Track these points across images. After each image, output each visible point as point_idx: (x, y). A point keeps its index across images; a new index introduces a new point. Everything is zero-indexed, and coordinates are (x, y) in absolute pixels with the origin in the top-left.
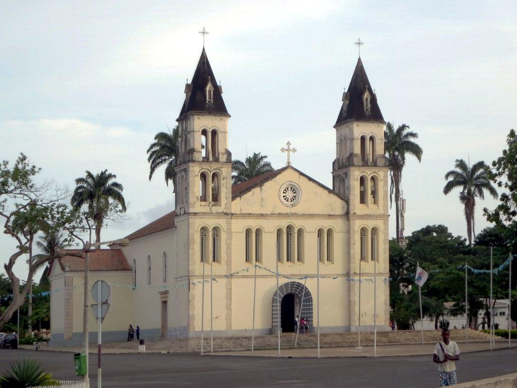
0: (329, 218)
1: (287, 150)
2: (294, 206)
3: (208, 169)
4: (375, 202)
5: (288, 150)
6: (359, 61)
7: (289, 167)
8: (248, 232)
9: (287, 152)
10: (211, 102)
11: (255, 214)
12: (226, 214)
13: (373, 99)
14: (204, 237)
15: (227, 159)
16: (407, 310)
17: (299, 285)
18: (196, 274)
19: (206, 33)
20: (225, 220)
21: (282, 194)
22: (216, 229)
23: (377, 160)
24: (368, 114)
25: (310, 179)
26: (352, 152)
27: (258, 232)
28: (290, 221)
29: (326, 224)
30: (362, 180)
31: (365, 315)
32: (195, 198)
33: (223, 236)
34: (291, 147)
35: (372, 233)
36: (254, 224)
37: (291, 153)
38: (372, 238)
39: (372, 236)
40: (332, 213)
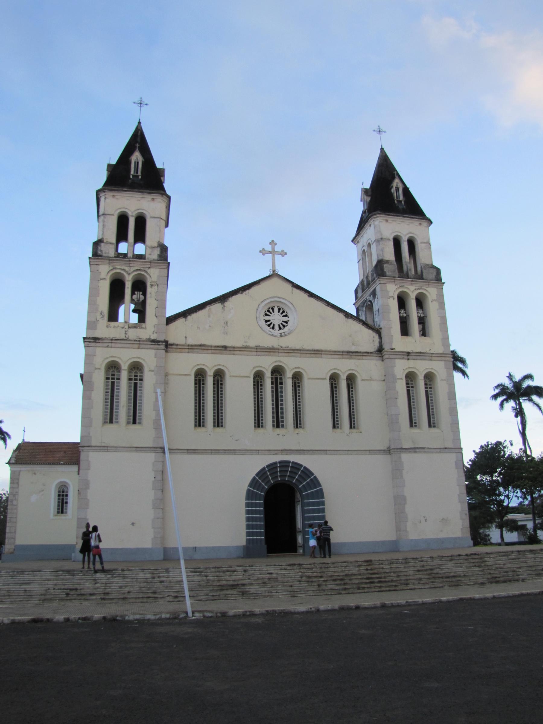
0: (349, 356)
1: (270, 252)
2: (285, 335)
3: (124, 270)
4: (424, 333)
5: (273, 252)
6: (381, 152)
7: (274, 275)
9: (271, 255)
10: (138, 176)
11: (211, 346)
12: (153, 341)
13: (406, 191)
14: (116, 381)
16: (505, 496)
17: (296, 466)
18: (93, 443)
20: (153, 351)
21: (263, 318)
23: (424, 271)
24: (400, 207)
25: (311, 295)
26: (380, 258)
27: (219, 376)
28: (278, 358)
30: (402, 302)
31: (426, 521)
32: (99, 314)
34: (277, 249)
35: (426, 384)
37: (277, 257)
38: (427, 392)
39: (426, 388)
40: (353, 349)
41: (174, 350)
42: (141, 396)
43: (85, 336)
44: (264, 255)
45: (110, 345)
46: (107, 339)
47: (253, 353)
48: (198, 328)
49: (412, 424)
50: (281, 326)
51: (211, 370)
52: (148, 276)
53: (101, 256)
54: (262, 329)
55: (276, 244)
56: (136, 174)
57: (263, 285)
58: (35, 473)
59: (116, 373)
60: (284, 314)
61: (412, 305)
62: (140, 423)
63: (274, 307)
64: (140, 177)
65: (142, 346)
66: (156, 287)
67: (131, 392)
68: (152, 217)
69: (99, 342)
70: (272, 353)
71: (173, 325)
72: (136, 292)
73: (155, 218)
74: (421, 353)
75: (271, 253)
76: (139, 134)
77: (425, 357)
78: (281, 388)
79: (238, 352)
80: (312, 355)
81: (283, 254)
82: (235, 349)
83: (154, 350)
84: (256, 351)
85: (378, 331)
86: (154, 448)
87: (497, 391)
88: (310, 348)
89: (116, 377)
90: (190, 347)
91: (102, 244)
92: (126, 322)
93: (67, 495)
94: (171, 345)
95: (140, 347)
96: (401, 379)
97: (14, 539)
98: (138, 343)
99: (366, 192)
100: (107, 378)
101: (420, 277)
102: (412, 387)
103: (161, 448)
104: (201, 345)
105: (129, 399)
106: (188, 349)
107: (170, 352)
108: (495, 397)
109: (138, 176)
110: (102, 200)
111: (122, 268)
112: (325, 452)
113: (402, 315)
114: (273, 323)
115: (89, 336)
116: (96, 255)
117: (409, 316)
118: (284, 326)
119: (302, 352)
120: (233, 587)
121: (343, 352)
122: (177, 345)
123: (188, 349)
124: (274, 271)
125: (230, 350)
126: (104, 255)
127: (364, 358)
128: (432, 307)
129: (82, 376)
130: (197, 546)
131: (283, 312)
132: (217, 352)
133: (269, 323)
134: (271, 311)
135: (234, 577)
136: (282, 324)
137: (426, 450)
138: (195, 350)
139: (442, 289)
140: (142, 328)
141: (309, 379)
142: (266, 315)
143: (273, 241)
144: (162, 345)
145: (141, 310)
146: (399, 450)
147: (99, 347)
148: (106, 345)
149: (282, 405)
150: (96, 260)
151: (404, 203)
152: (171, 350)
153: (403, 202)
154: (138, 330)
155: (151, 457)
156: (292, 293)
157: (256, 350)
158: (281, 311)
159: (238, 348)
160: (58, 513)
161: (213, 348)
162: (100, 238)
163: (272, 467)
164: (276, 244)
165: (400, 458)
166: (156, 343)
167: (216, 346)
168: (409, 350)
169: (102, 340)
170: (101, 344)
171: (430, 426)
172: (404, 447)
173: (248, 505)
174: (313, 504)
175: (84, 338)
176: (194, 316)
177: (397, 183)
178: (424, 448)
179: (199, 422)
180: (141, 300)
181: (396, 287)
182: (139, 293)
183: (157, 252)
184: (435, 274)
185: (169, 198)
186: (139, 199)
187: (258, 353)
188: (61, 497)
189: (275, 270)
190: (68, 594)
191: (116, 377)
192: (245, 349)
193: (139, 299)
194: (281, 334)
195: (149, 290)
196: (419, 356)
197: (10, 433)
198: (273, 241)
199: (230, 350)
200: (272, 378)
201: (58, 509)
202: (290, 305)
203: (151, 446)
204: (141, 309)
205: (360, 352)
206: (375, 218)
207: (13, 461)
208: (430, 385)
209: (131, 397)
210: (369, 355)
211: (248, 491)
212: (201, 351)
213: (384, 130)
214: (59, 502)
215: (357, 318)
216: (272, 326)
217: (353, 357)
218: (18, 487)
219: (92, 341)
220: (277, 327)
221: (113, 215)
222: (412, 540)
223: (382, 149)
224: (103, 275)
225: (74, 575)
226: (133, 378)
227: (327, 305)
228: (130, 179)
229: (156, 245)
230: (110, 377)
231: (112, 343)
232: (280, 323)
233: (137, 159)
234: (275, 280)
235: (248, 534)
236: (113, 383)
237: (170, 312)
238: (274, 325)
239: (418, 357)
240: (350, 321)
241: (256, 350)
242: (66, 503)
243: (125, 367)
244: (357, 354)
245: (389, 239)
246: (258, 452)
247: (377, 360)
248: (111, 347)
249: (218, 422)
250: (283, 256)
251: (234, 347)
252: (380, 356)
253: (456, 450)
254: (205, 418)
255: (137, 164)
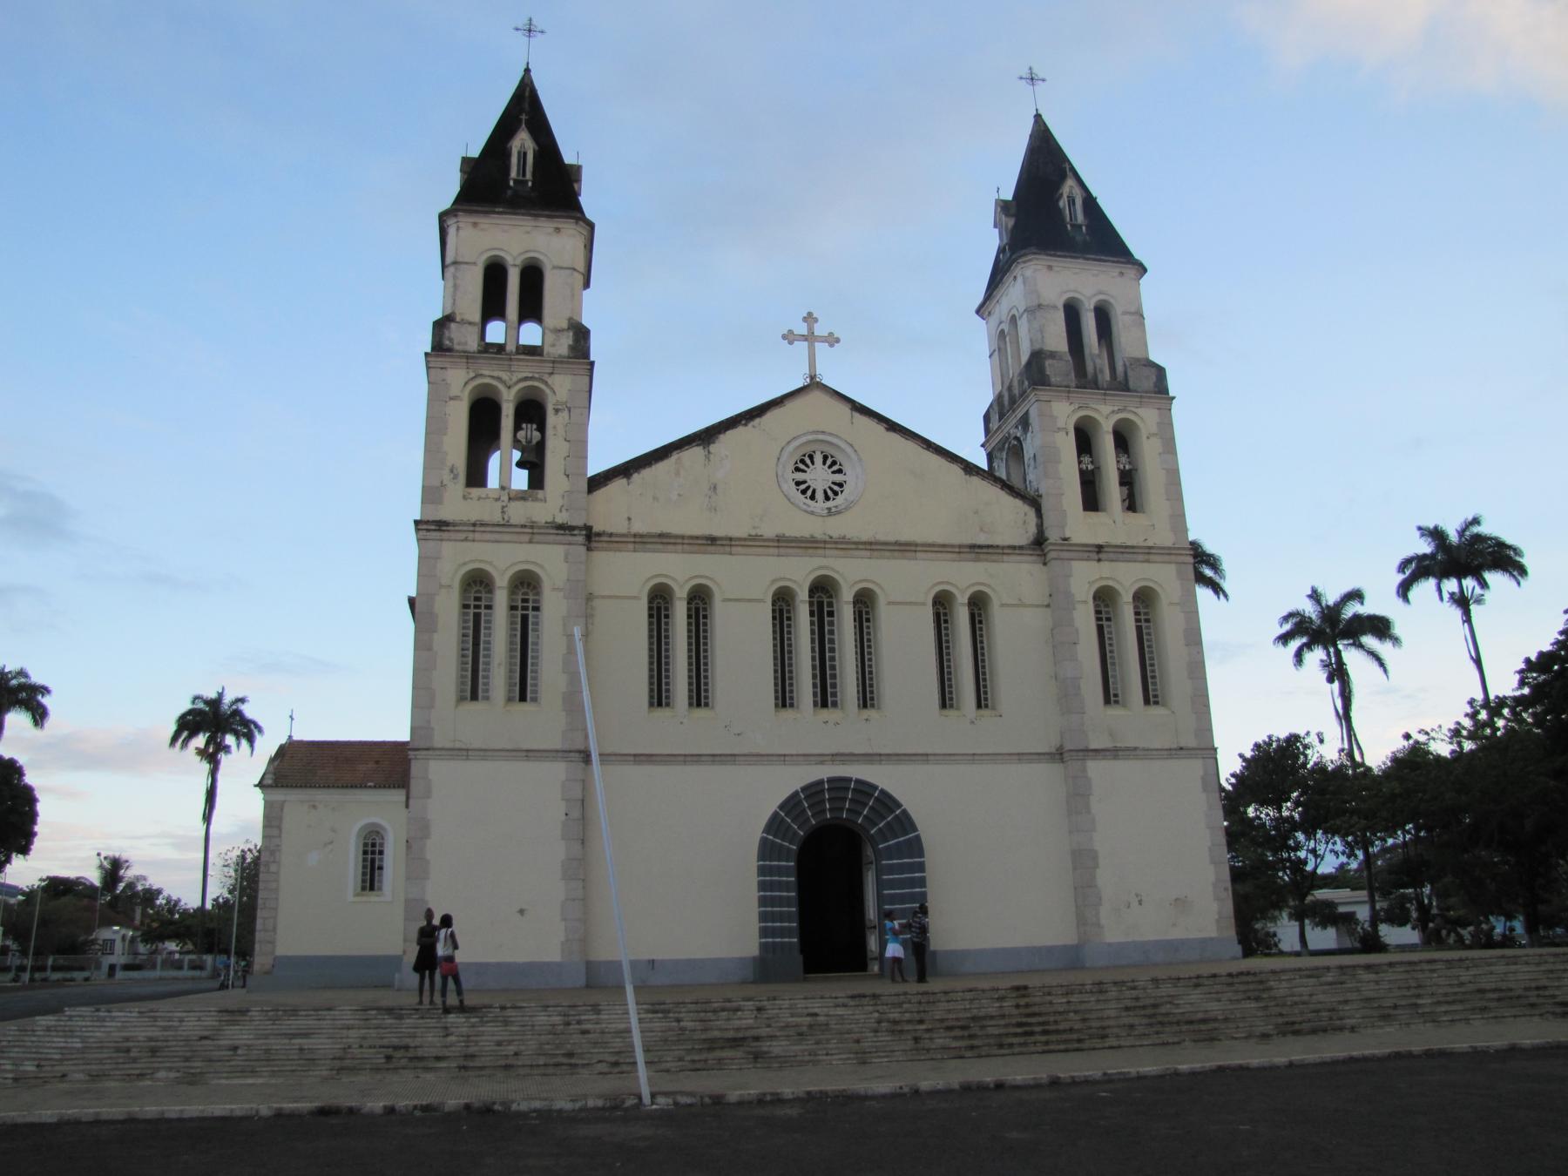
0: (973, 555)
1: (804, 338)
2: (839, 513)
3: (499, 379)
4: (1132, 504)
5: (810, 338)
7: (814, 385)
8: (659, 601)
9: (806, 343)
10: (527, 181)
11: (683, 537)
13: (1090, 203)
14: (483, 611)
15: (572, 348)
18: (438, 743)
19: (530, 24)
22: (526, 583)
23: (1130, 373)
24: (1079, 238)
26: (1037, 347)
27: (700, 600)
29: (963, 578)
30: (1085, 440)
31: (1140, 903)
32: (447, 471)
33: (553, 608)
34: (820, 330)
35: (1137, 613)
36: (680, 571)
37: (821, 348)
38: (1139, 630)
39: (1137, 621)
41: (605, 545)
42: (536, 644)
43: (419, 518)
44: (791, 343)
45: (471, 536)
46: (464, 524)
47: (771, 550)
48: (655, 498)
49: (1109, 697)
50: (829, 492)
51: (681, 587)
52: (548, 391)
53: (450, 350)
54: (789, 500)
55: (816, 320)
56: (521, 178)
57: (790, 406)
58: (314, 807)
59: (483, 595)
60: (835, 468)
61: (1107, 445)
62: (534, 700)
63: (814, 452)
64: (530, 184)
65: (537, 538)
66: (565, 414)
67: (515, 635)
68: (555, 267)
69: (448, 531)
70: (810, 551)
71: (601, 494)
72: (524, 426)
73: (561, 268)
74: (1127, 547)
75: (806, 340)
76: (527, 94)
77: (1135, 556)
78: (831, 624)
79: (739, 549)
80: (896, 554)
81: (832, 340)
82: (733, 543)
83: (562, 547)
84: (778, 547)
85: (1035, 502)
86: (566, 751)
87: (1287, 627)
88: (891, 539)
89: (483, 603)
90: (637, 540)
91: (453, 325)
92: (503, 488)
93: (381, 853)
94: (599, 535)
95: (535, 540)
96: (1085, 602)
97: (273, 942)
98: (530, 531)
99: (1004, 207)
100: (466, 606)
101: (1121, 386)
102: (1108, 619)
103: (580, 752)
104: (661, 535)
105: (511, 650)
106: (634, 542)
107: (597, 549)
108: (1284, 639)
109: (527, 181)
110: (452, 232)
111: (496, 374)
112: (925, 758)
113: (1084, 467)
114: (813, 486)
115: (426, 518)
116: (440, 347)
117: (1098, 468)
118: (836, 493)
119: (874, 547)
120: (735, 1042)
121: (960, 546)
122: (611, 535)
123: (634, 542)
124: (812, 377)
125: (722, 545)
126: (457, 347)
127: (1005, 557)
128: (1147, 449)
129: (412, 602)
130: (655, 958)
131: (834, 463)
132: (696, 548)
133: (803, 487)
134: (808, 461)
135: (737, 1023)
136: (830, 488)
137: (1138, 752)
138: (649, 546)
139: (1170, 410)
140: (536, 500)
141: (889, 603)
142: (797, 469)
143: (810, 314)
144: (580, 535)
145: (534, 463)
146: (1081, 754)
147: (449, 540)
148: (462, 536)
149: (833, 659)
150: (440, 359)
151: (1086, 229)
152: (599, 545)
153: (1084, 228)
154: (529, 504)
155: (558, 771)
156: (852, 423)
157: (776, 544)
158: (829, 462)
159: (740, 539)
160: (363, 889)
161: (686, 541)
162: (448, 312)
163: (813, 791)
164: (816, 320)
165: (1084, 770)
166: (567, 532)
167: (691, 537)
168: (1100, 541)
169: (454, 526)
170: (453, 535)
171: (1147, 701)
172: (1093, 746)
173: (762, 871)
174: (902, 868)
175: (416, 523)
176: (647, 473)
177: (1071, 187)
178: (1135, 749)
179: (659, 696)
180: (534, 442)
181: (1072, 408)
182: (529, 426)
183: (567, 340)
184: (1154, 378)
185: (591, 226)
186: (529, 229)
187: (782, 551)
188: (369, 856)
189: (815, 375)
190: (389, 1058)
191: (483, 603)
192: (753, 542)
193: (531, 439)
194: (829, 509)
195: (551, 420)
196: (1122, 553)
197: (260, 723)
198: (810, 314)
199: (722, 545)
200: (811, 604)
201: (364, 881)
202: (849, 450)
203: (559, 747)
204: (535, 460)
205: (998, 547)
206: (1024, 262)
207: (269, 781)
208: (1146, 614)
209: (516, 644)
210: (1017, 551)
211: (764, 842)
212: (661, 547)
213: (1041, 76)
214: (364, 867)
215: (989, 475)
216: (809, 493)
217: (982, 556)
218: (280, 836)
219: (433, 527)
220: (820, 495)
221: (475, 264)
222: (1110, 945)
223: (1038, 117)
224: (455, 391)
225: (400, 1017)
226: (520, 604)
227: (925, 447)
228: (510, 188)
229: (565, 325)
230: (472, 603)
231: (474, 531)
232: (826, 487)
233: (523, 146)
234: (816, 396)
235: (764, 932)
236: (477, 617)
237: (595, 467)
238: (814, 491)
239: (1120, 556)
240: (976, 480)
241: (776, 544)
242: (381, 868)
243: (502, 582)
244: (990, 551)
245: (1055, 307)
246: (782, 758)
247: (1034, 562)
248: (474, 541)
249: (699, 697)
250: (832, 346)
251: (731, 539)
252: (1038, 555)
253: (1204, 752)
254: (671, 687)
255: (523, 156)
